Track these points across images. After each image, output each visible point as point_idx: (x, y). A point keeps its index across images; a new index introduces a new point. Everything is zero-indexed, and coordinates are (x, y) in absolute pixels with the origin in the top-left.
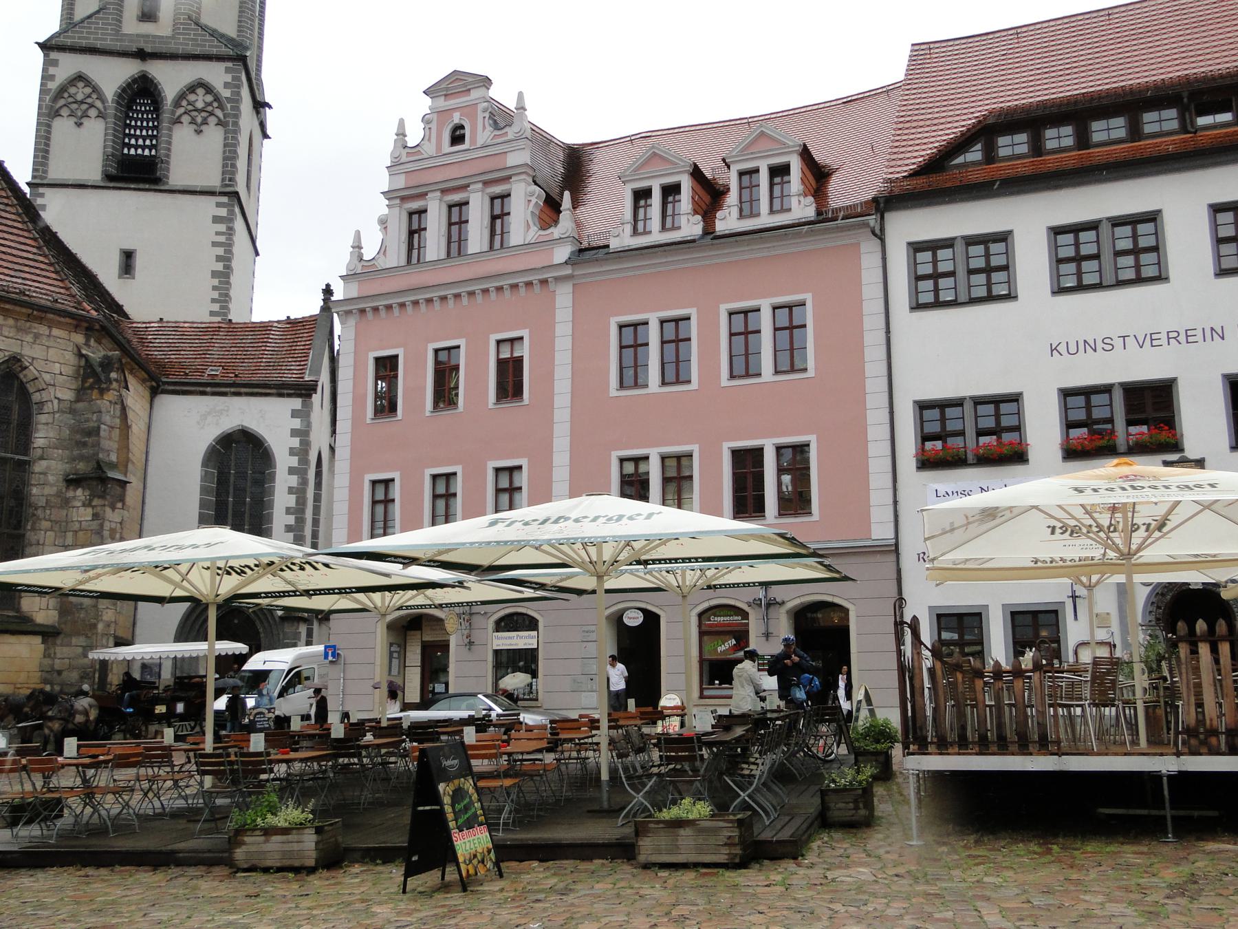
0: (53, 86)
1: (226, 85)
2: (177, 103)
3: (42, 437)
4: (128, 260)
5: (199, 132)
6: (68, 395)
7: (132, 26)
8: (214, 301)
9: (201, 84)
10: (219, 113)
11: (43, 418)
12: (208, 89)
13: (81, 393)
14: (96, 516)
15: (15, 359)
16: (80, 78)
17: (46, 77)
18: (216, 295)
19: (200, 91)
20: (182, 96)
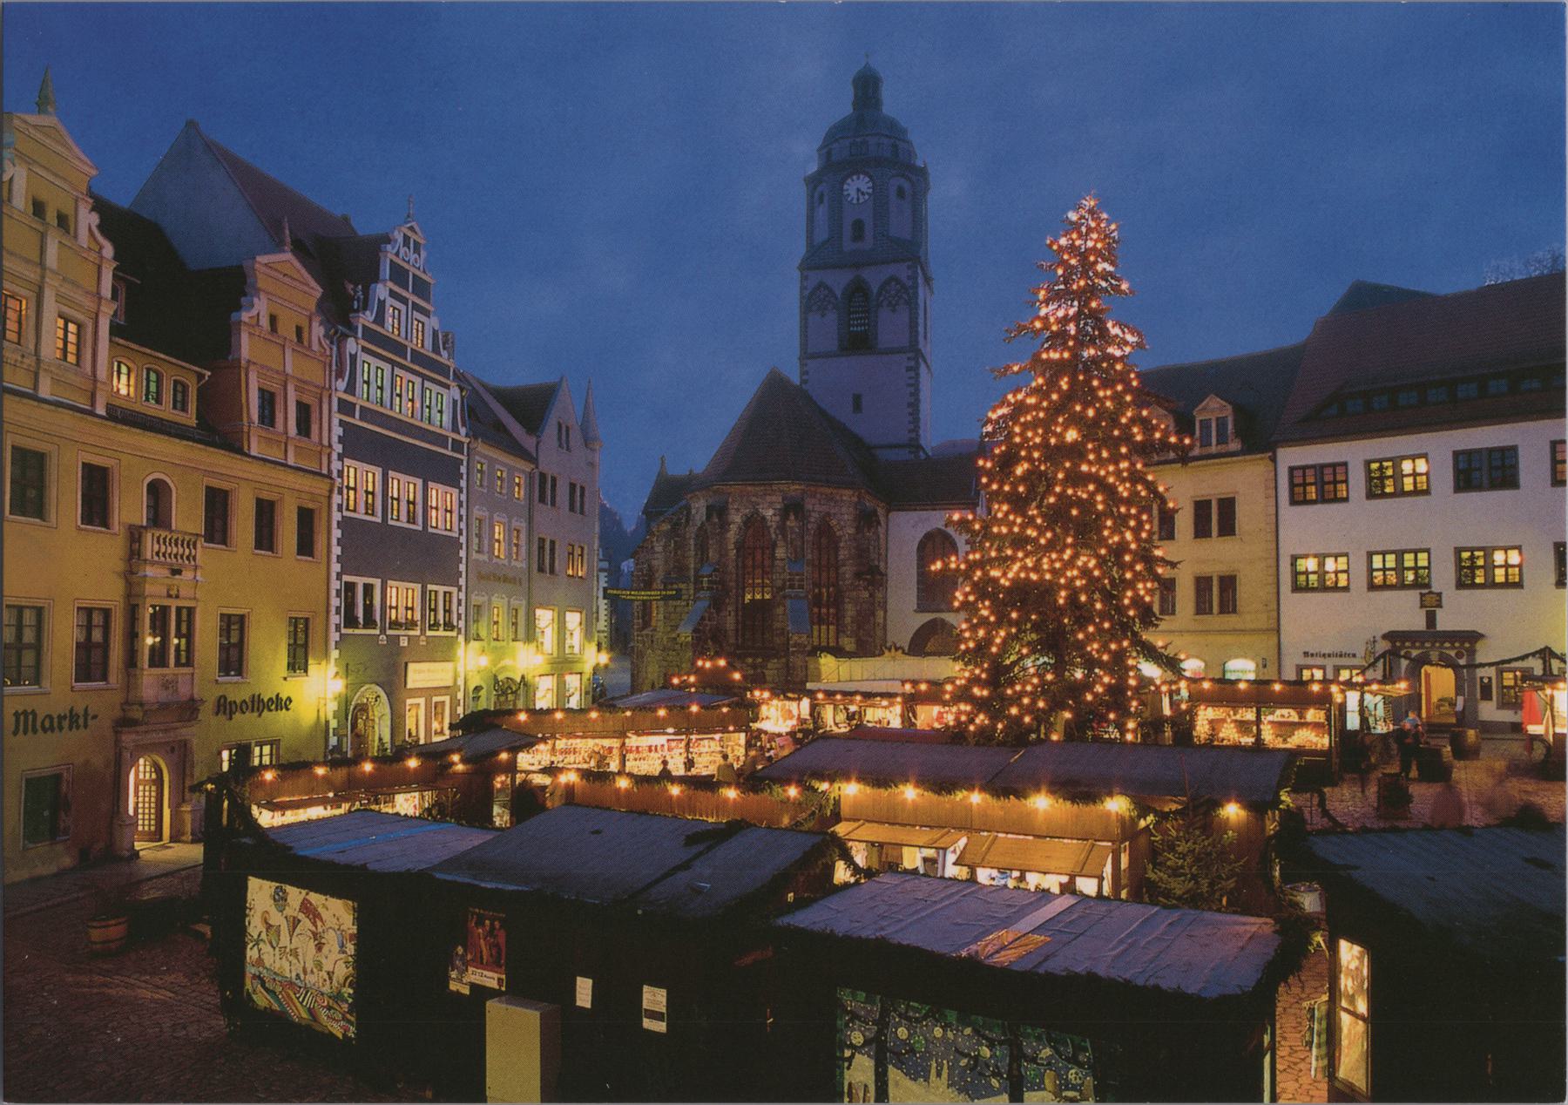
0: (807, 293)
1: (909, 278)
2: (879, 294)
3: (843, 554)
4: (857, 404)
5: (894, 311)
6: (851, 531)
7: (848, 245)
8: (910, 422)
9: (892, 279)
10: (905, 296)
11: (842, 545)
12: (898, 281)
13: (858, 529)
14: (871, 595)
15: (828, 514)
16: (821, 285)
17: (803, 288)
18: (911, 418)
19: (893, 283)
20: (882, 287)
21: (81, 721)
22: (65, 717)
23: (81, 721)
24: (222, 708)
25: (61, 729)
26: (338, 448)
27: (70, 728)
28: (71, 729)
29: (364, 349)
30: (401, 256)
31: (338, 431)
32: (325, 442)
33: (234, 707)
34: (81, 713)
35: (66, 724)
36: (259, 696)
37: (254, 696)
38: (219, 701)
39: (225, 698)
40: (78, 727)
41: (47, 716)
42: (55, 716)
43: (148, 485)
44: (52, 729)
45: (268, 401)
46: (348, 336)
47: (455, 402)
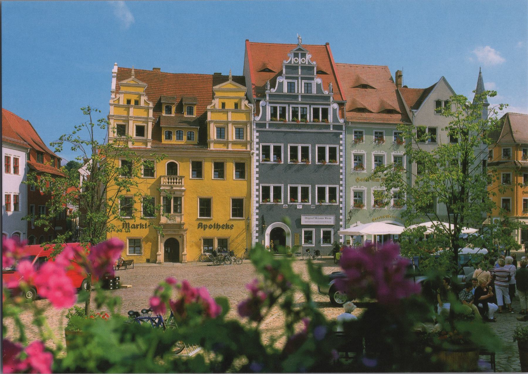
21: (144, 226)
22: (139, 225)
23: (144, 226)
24: (200, 228)
25: (137, 228)
26: (256, 140)
27: (141, 228)
28: (141, 228)
29: (270, 103)
30: (293, 63)
31: (256, 134)
32: (249, 139)
33: (206, 226)
34: (144, 224)
35: (139, 227)
36: (217, 224)
37: (215, 224)
38: (199, 224)
39: (202, 224)
40: (143, 228)
41: (211, 228)
42: (136, 225)
43: (168, 164)
44: (135, 228)
45: (221, 132)
46: (261, 100)
47: (334, 110)
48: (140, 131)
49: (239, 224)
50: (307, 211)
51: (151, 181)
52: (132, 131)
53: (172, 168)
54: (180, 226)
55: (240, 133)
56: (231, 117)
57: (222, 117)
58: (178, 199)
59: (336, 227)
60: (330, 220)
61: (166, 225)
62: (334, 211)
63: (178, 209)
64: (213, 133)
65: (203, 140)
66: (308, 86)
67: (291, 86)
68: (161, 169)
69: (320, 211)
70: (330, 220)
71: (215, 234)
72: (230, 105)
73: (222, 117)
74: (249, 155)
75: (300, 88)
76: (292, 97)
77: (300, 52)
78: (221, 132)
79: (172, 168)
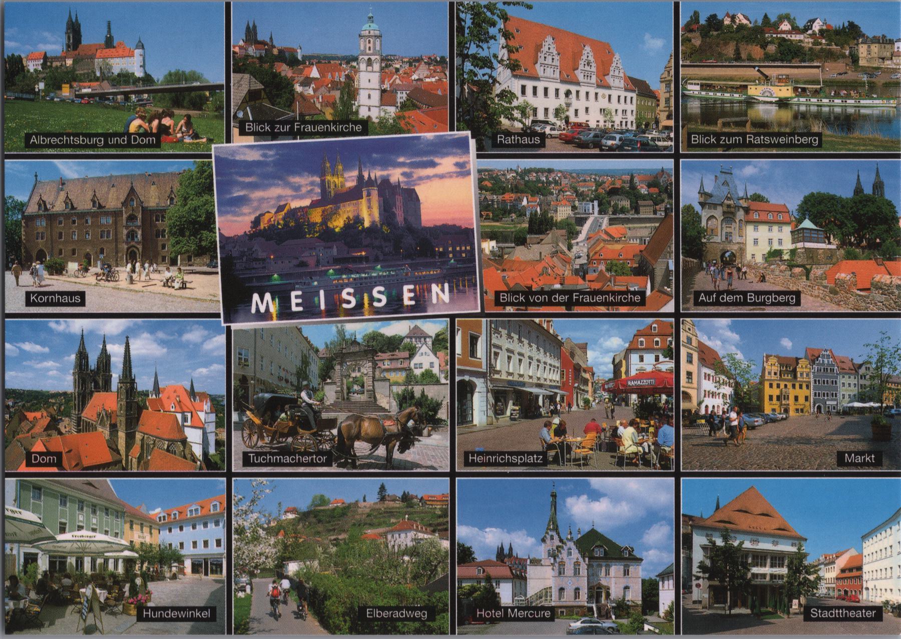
45: (802, 374)
48: (775, 374)
49: (807, 404)
50: (828, 400)
51: (778, 390)
52: (773, 373)
53: (786, 386)
54: (788, 405)
55: (808, 375)
56: (804, 370)
57: (802, 370)
58: (788, 396)
59: (837, 405)
60: (835, 403)
61: (785, 404)
62: (836, 400)
63: (788, 399)
64: (799, 375)
65: (795, 377)
66: (828, 361)
67: (823, 361)
68: (782, 386)
69: (832, 400)
70: (835, 403)
71: (800, 407)
72: (804, 366)
73: (802, 370)
74: (810, 382)
75: (826, 361)
76: (823, 364)
77: (826, 350)
78: (802, 374)
79: (786, 386)
